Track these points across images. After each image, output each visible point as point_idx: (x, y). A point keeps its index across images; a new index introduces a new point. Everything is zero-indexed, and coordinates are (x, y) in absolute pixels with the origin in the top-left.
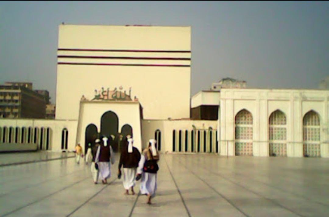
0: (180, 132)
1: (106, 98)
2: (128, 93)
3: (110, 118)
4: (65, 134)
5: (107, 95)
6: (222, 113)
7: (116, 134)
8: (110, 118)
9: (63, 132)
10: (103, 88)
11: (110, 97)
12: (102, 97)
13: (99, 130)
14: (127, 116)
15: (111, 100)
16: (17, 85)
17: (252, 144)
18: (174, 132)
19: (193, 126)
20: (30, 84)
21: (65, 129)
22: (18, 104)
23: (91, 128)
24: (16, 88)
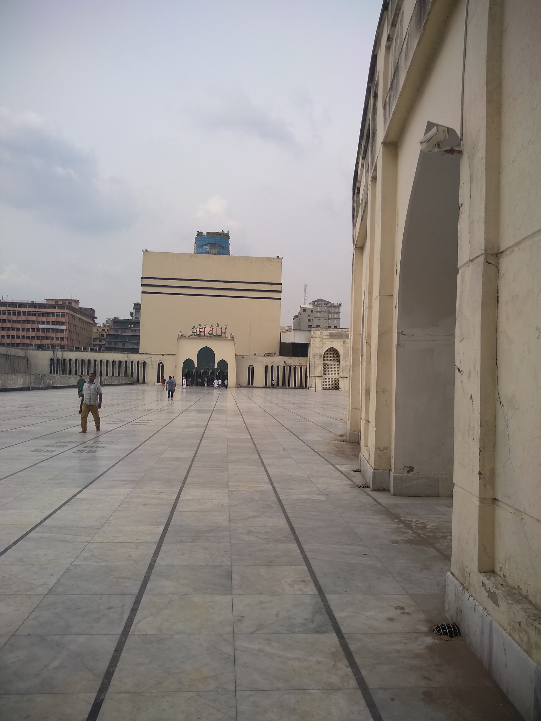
0: (272, 367)
1: (203, 334)
2: (224, 331)
3: (206, 354)
5: (204, 332)
6: (312, 350)
8: (206, 354)
10: (200, 325)
12: (198, 333)
13: (196, 366)
14: (223, 352)
15: (206, 336)
16: (60, 303)
19: (285, 362)
20: (77, 302)
23: (188, 363)
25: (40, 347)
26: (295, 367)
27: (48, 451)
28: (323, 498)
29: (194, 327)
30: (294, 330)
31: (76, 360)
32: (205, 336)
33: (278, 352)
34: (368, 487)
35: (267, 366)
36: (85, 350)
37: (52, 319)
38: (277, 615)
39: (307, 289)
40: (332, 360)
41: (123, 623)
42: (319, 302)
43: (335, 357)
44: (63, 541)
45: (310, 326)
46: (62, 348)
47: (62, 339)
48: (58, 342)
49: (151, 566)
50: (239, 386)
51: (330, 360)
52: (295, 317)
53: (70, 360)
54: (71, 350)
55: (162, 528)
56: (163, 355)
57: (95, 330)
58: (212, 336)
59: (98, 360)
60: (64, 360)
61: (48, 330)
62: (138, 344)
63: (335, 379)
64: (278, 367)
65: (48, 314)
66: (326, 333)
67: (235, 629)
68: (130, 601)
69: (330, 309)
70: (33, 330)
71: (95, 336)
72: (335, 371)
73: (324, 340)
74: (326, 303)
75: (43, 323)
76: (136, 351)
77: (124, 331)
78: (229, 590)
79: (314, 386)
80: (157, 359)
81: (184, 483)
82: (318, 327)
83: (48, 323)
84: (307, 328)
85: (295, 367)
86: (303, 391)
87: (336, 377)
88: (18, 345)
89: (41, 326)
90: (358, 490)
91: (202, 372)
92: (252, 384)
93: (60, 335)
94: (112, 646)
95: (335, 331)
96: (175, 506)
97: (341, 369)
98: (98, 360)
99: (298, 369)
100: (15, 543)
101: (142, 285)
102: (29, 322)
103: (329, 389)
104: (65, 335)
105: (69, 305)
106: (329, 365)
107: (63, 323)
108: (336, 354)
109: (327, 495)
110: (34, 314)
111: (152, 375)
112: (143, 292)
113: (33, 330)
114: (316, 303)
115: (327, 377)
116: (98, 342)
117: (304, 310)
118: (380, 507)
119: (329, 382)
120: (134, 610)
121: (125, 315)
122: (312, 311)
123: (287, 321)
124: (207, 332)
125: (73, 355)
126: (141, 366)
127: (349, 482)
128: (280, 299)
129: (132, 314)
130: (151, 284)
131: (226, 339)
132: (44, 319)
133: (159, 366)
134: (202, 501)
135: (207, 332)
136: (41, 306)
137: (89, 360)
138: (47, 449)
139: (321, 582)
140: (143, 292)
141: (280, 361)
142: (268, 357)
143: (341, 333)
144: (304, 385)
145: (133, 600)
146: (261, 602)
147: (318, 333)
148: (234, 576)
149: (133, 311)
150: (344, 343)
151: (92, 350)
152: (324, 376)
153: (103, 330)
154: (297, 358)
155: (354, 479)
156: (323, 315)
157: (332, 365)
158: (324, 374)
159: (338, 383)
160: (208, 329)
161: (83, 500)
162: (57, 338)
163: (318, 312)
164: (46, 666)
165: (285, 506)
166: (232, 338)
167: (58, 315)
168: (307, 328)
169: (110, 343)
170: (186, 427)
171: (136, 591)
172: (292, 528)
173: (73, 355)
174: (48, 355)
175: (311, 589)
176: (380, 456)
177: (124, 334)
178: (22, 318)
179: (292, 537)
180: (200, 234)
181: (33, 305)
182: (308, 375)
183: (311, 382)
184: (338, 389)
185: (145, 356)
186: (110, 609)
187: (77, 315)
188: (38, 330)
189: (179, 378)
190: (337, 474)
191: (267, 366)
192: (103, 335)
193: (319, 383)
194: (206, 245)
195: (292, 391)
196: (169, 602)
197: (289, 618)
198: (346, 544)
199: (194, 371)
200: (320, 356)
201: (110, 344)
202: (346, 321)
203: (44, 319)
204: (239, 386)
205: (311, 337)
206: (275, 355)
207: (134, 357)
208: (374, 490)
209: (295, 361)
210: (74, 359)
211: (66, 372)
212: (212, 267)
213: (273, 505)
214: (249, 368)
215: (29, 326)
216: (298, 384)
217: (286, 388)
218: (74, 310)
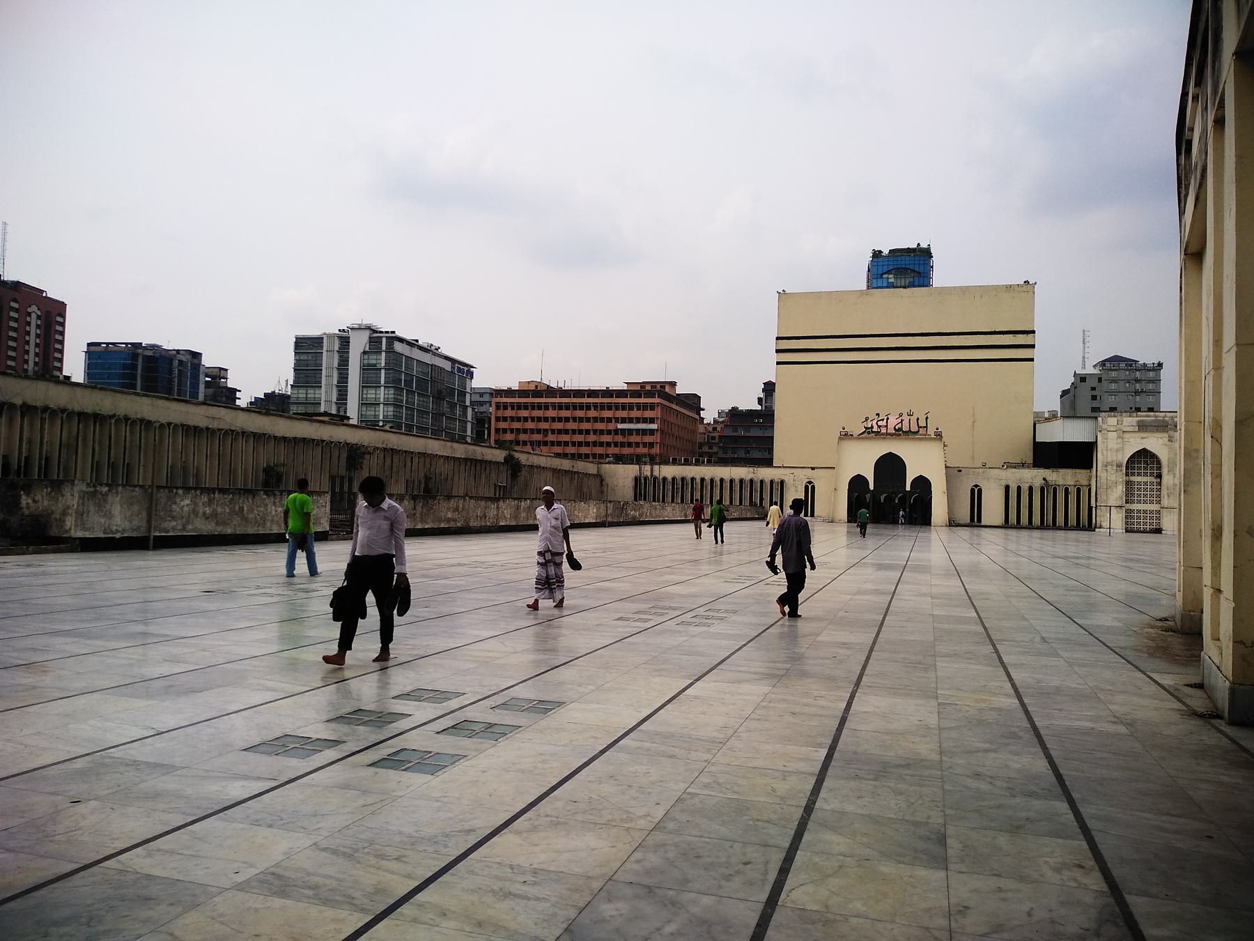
0: (1019, 488)
1: (883, 430)
2: (922, 423)
3: (890, 466)
6: (1101, 456)
8: (890, 466)
13: (871, 487)
14: (921, 461)
15: (891, 435)
16: (648, 388)
20: (673, 384)
22: (654, 426)
23: (857, 483)
24: (650, 394)
25: (619, 459)
26: (1067, 489)
27: (639, 620)
28: (1122, 729)
29: (867, 419)
30: (1063, 417)
31: (673, 479)
32: (887, 434)
33: (1030, 461)
34: (1220, 717)
35: (1007, 488)
36: (687, 463)
37: (635, 413)
38: (1029, 914)
39: (1087, 339)
40: (1146, 475)
41: (768, 888)
42: (1114, 363)
43: (1152, 468)
44: (671, 757)
45: (1095, 410)
46: (653, 461)
47: (651, 445)
48: (645, 450)
49: (809, 809)
50: (952, 523)
51: (1139, 474)
52: (1064, 393)
53: (665, 479)
54: (666, 463)
55: (824, 752)
56: (813, 469)
57: (701, 429)
58: (899, 433)
59: (707, 478)
60: (655, 478)
61: (630, 431)
62: (771, 450)
63: (1151, 512)
64: (1031, 488)
65: (631, 407)
66: (1130, 421)
67: (953, 924)
68: (777, 858)
69: (1138, 374)
70: (609, 432)
71: (699, 439)
72: (1152, 496)
73: (1127, 435)
74: (1130, 363)
75: (623, 421)
76: (768, 462)
77: (747, 429)
78: (942, 862)
79: (1105, 524)
80: (803, 476)
81: (858, 684)
82: (1113, 409)
83: (631, 420)
84: (1090, 414)
85: (1067, 489)
86: (1083, 535)
87: (1154, 507)
88: (587, 456)
89: (620, 426)
90: (1195, 722)
91: (882, 498)
92: (979, 520)
93: (648, 439)
94: (753, 919)
95: (1150, 417)
96: (843, 721)
97: (1164, 492)
98: (707, 478)
99: (1073, 491)
100: (603, 752)
101: (777, 351)
102: (602, 420)
103: (1139, 531)
104: (656, 438)
105: (661, 391)
106: (1139, 483)
107: (652, 421)
109: (1131, 724)
110: (610, 408)
112: (778, 363)
113: (609, 432)
114: (1108, 365)
115: (1135, 507)
116: (706, 449)
117: (1083, 379)
118: (1245, 755)
119: (1139, 518)
120: (784, 871)
121: (749, 401)
122: (1100, 380)
123: (1050, 401)
124: (891, 426)
125: (668, 471)
126: (776, 487)
127: (1177, 705)
128: (1032, 360)
129: (760, 400)
130: (792, 349)
131: (926, 438)
132: (623, 414)
133: (806, 487)
134: (891, 717)
135: (891, 426)
136: (620, 393)
137: (693, 479)
138: (637, 616)
139: (1116, 872)
140: (778, 363)
141: (1034, 477)
142: (1010, 470)
145: (782, 856)
146: (1000, 889)
147: (1112, 421)
148: (949, 841)
149: (762, 395)
150: (1171, 440)
151: (698, 463)
153: (715, 429)
154: (1069, 472)
155: (1188, 701)
156: (1122, 386)
157: (1146, 483)
158: (1127, 502)
159: (1159, 518)
160: (893, 422)
161: (696, 697)
162: (645, 445)
163: (1114, 381)
164: (658, 929)
165: (1045, 738)
166: (939, 436)
167: (644, 407)
168: (1090, 414)
169: (725, 449)
170: (858, 593)
171: (787, 845)
172: (1059, 777)
173: (668, 471)
174: (631, 471)
175: (1095, 881)
176: (1243, 658)
177: (749, 434)
178: (592, 413)
179: (1059, 790)
180: (877, 254)
181: (608, 393)
183: (1102, 517)
184: (1158, 531)
185: (782, 471)
186: (746, 864)
187: (674, 406)
188: (617, 431)
189: (842, 510)
190: (1154, 687)
191: (1007, 488)
192: (713, 438)
193: (1118, 520)
194: (889, 272)
195: (1061, 534)
196: (841, 867)
197: (1053, 922)
198: (1168, 814)
199: (868, 496)
200: (1119, 466)
201: (725, 453)
202: (1171, 396)
203: (623, 414)
204: (952, 523)
205: (1097, 429)
206: (1023, 465)
207: (765, 473)
208: (1232, 723)
209: (1064, 477)
210: (670, 478)
212: (902, 309)
213: (1021, 734)
214: (972, 491)
215: (601, 426)
216: (1072, 520)
217: (1047, 528)
218: (669, 398)
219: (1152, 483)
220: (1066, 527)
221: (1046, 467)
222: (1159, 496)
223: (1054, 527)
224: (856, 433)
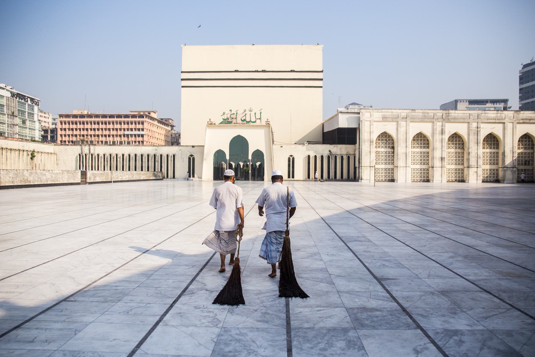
2: (258, 116)
3: (240, 144)
4: (191, 160)
7: (246, 161)
8: (240, 144)
9: (189, 159)
10: (231, 110)
11: (239, 121)
12: (230, 120)
13: (228, 157)
17: (393, 169)
18: (309, 156)
19: (330, 151)
21: (192, 155)
26: (342, 157)
33: (321, 140)
43: (389, 143)
64: (322, 157)
66: (377, 115)
73: (375, 123)
87: (391, 166)
92: (293, 177)
108: (389, 140)
111: (182, 168)
125: (100, 150)
141: (324, 149)
143: (396, 115)
144: (354, 177)
152: (377, 166)
159: (393, 173)
166: (268, 124)
173: (100, 150)
182: (357, 165)
191: (309, 156)
205: (359, 120)
211: (95, 168)
214: (289, 159)
217: (332, 180)
219: (389, 152)
220: (342, 179)
221: (330, 144)
222: (393, 160)
223: (335, 179)
224: (217, 124)
